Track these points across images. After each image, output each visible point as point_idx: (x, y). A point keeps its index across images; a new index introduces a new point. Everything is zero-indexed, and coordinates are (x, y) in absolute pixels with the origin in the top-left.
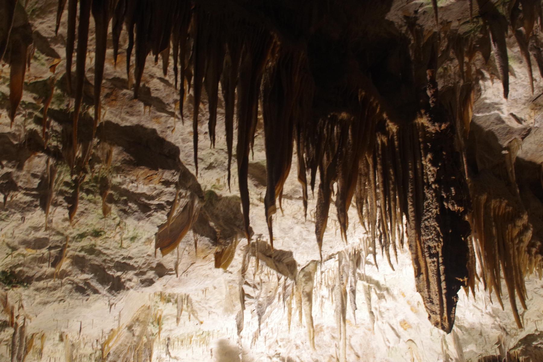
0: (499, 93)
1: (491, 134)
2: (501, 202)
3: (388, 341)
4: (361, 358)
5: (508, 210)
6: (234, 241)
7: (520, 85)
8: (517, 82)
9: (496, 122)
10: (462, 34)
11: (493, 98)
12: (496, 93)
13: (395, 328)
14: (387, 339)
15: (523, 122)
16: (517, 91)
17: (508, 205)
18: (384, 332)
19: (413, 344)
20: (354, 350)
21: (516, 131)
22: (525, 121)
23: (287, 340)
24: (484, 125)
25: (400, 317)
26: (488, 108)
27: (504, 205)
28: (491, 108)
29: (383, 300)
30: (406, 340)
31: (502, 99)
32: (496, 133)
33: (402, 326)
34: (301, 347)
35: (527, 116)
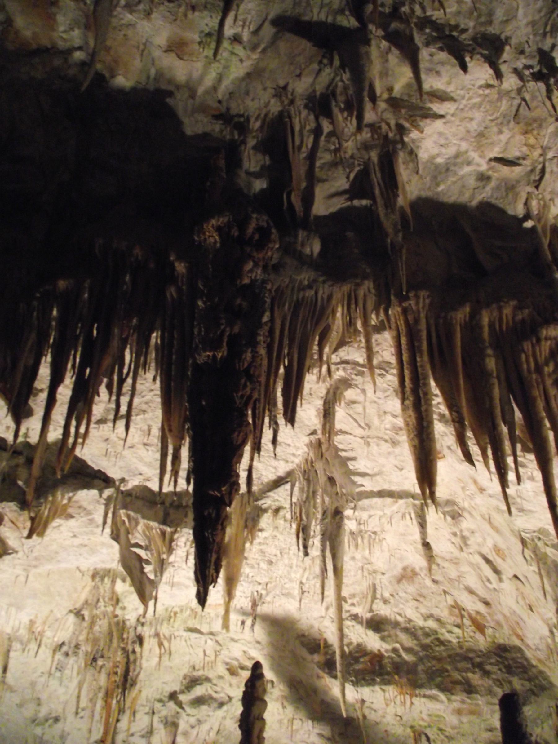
0: (447, 139)
1: (486, 207)
2: (500, 309)
3: (489, 580)
4: (493, 606)
5: (519, 317)
6: (50, 498)
7: (471, 108)
8: (461, 107)
9: (480, 184)
10: (324, 91)
11: (443, 150)
12: (442, 142)
13: (490, 557)
14: (486, 577)
15: (521, 161)
16: (472, 119)
18: (479, 568)
19: (518, 582)
20: (477, 595)
21: (518, 182)
22: (524, 159)
23: (361, 596)
24: (465, 198)
25: (490, 543)
26: (447, 170)
27: (507, 311)
28: (452, 168)
29: (461, 518)
30: (511, 575)
31: (459, 145)
32: (493, 201)
33: (498, 555)
34: (392, 600)
35: (525, 149)
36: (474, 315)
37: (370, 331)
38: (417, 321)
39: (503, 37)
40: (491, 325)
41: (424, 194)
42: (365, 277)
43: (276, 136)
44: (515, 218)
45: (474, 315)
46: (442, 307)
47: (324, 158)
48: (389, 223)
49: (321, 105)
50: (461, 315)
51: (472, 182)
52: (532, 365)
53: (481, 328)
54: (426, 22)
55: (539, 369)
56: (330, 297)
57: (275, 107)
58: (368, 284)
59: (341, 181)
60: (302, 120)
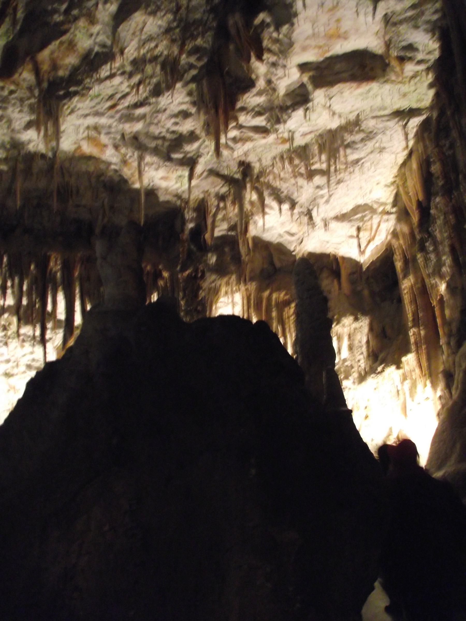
2: (279, 295)
17: (286, 294)
36: (271, 294)
37: (233, 293)
38: (250, 295)
39: (296, 201)
40: (276, 299)
41: (257, 235)
42: (232, 274)
43: (202, 208)
44: (289, 251)
45: (271, 294)
46: (260, 290)
47: (220, 216)
48: (243, 250)
49: (222, 198)
50: (266, 294)
51: (276, 236)
52: (287, 316)
53: (272, 301)
54: (269, 186)
55: (289, 318)
56: (220, 285)
57: (201, 196)
58: (234, 277)
59: (225, 226)
60: (213, 202)
